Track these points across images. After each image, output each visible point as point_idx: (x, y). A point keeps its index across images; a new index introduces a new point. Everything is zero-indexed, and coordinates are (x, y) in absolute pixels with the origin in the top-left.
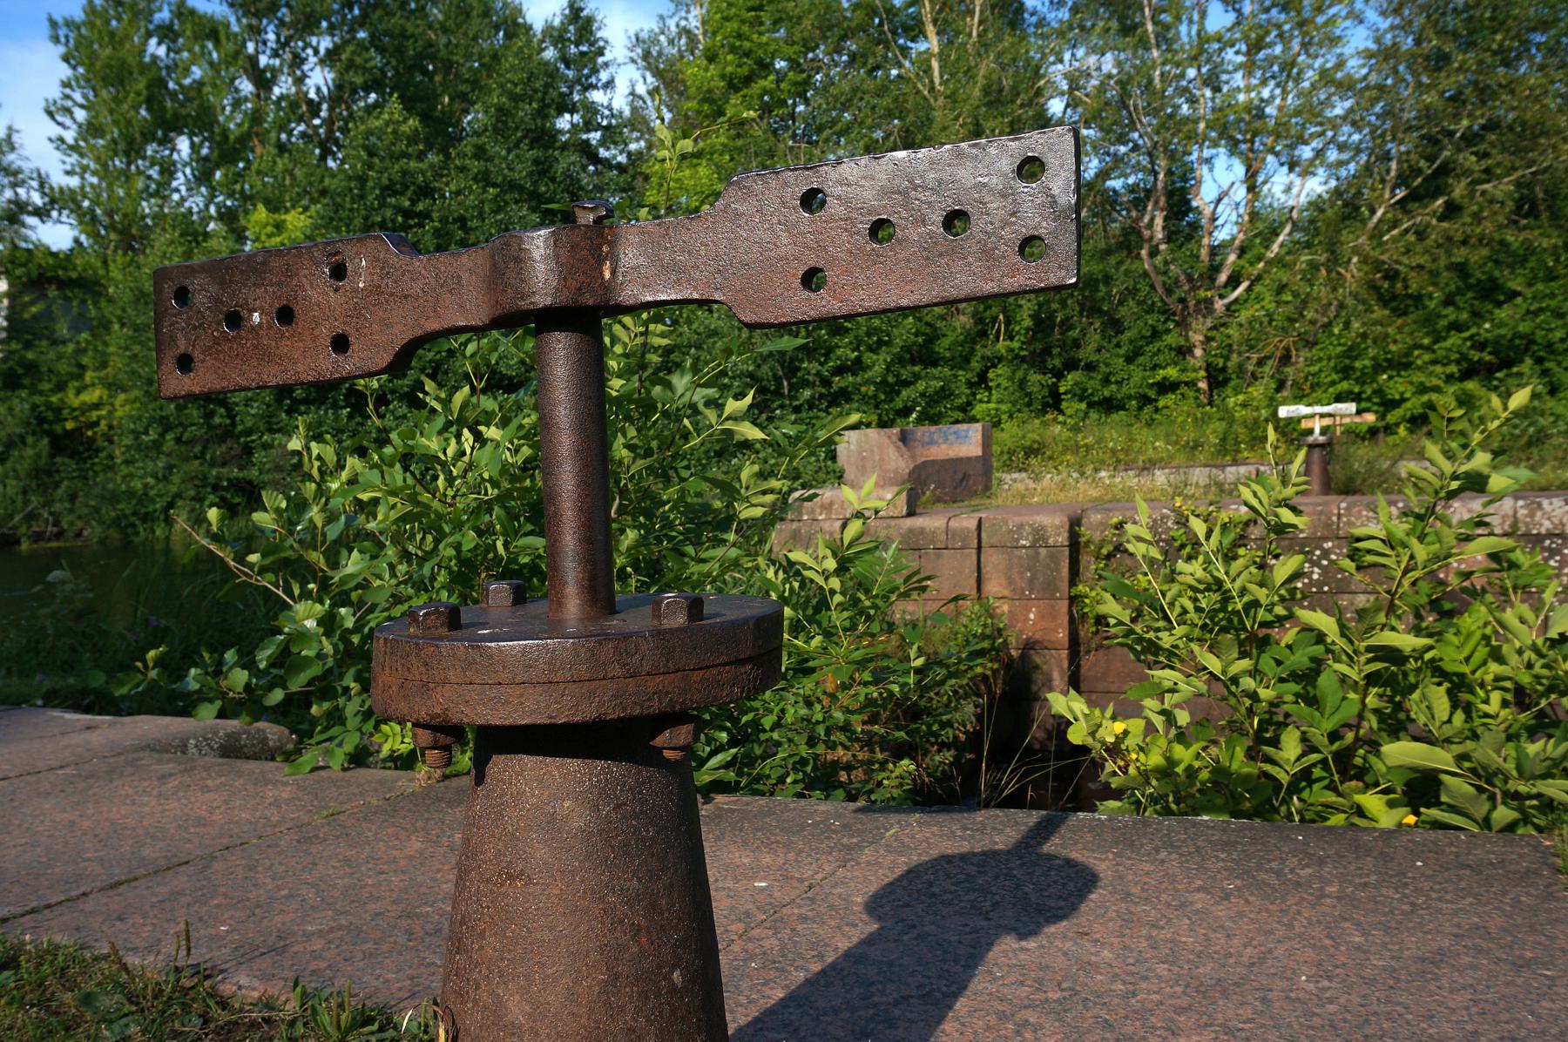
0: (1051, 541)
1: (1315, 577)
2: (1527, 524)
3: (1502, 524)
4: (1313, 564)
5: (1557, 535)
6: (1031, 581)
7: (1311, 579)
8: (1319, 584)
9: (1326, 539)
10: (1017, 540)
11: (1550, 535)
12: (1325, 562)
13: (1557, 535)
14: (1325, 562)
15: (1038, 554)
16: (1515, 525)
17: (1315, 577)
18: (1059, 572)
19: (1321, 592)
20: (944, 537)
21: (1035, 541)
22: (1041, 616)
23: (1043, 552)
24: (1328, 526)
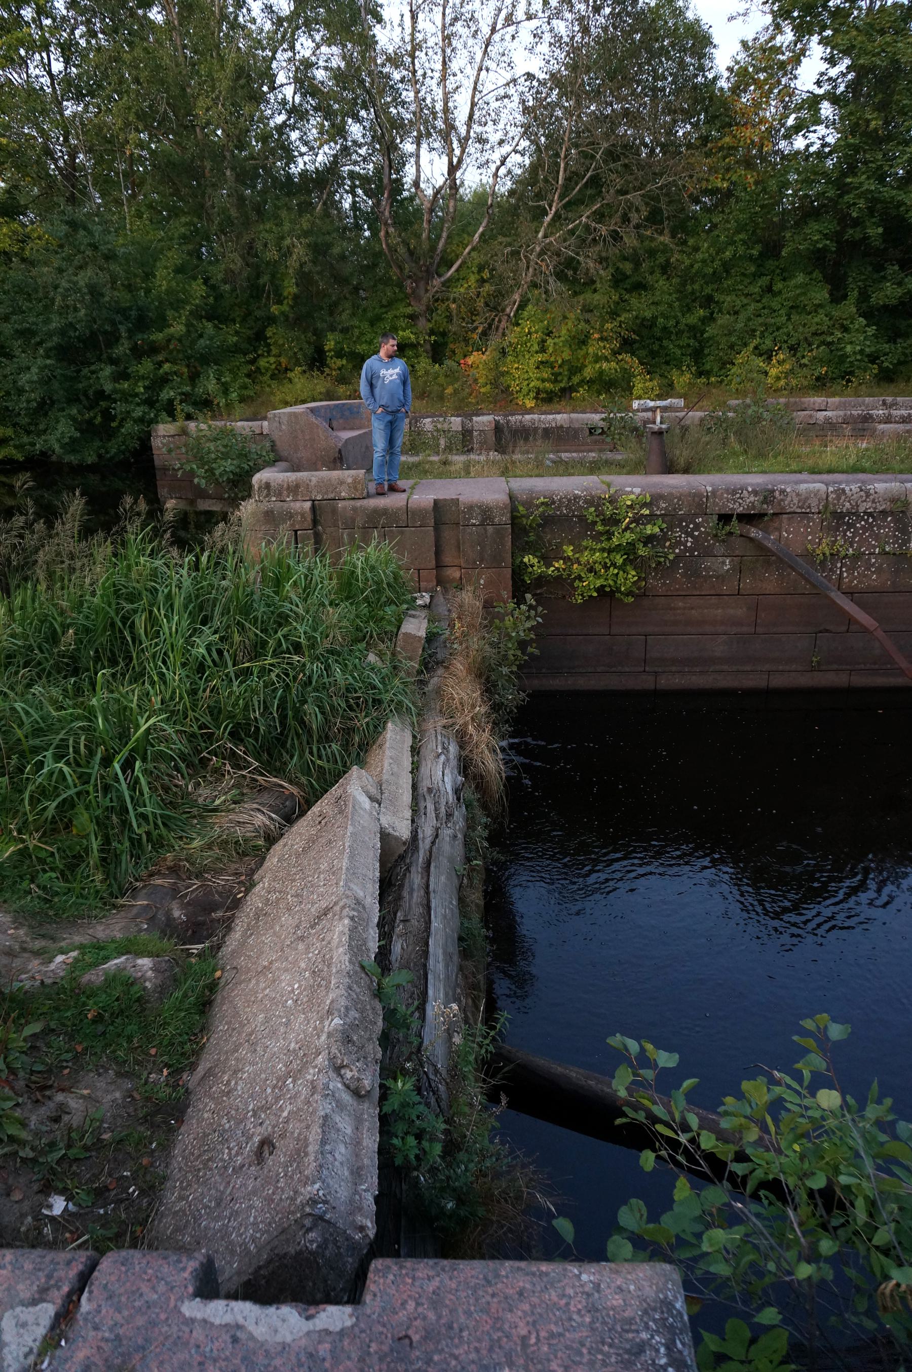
1: (689, 544)
2: (834, 505)
3: (818, 505)
4: (688, 534)
5: (853, 514)
7: (686, 546)
8: (691, 550)
9: (697, 515)
10: (469, 519)
11: (849, 513)
13: (853, 514)
15: (485, 530)
16: (826, 507)
17: (689, 544)
19: (692, 555)
23: (490, 529)
24: (699, 505)
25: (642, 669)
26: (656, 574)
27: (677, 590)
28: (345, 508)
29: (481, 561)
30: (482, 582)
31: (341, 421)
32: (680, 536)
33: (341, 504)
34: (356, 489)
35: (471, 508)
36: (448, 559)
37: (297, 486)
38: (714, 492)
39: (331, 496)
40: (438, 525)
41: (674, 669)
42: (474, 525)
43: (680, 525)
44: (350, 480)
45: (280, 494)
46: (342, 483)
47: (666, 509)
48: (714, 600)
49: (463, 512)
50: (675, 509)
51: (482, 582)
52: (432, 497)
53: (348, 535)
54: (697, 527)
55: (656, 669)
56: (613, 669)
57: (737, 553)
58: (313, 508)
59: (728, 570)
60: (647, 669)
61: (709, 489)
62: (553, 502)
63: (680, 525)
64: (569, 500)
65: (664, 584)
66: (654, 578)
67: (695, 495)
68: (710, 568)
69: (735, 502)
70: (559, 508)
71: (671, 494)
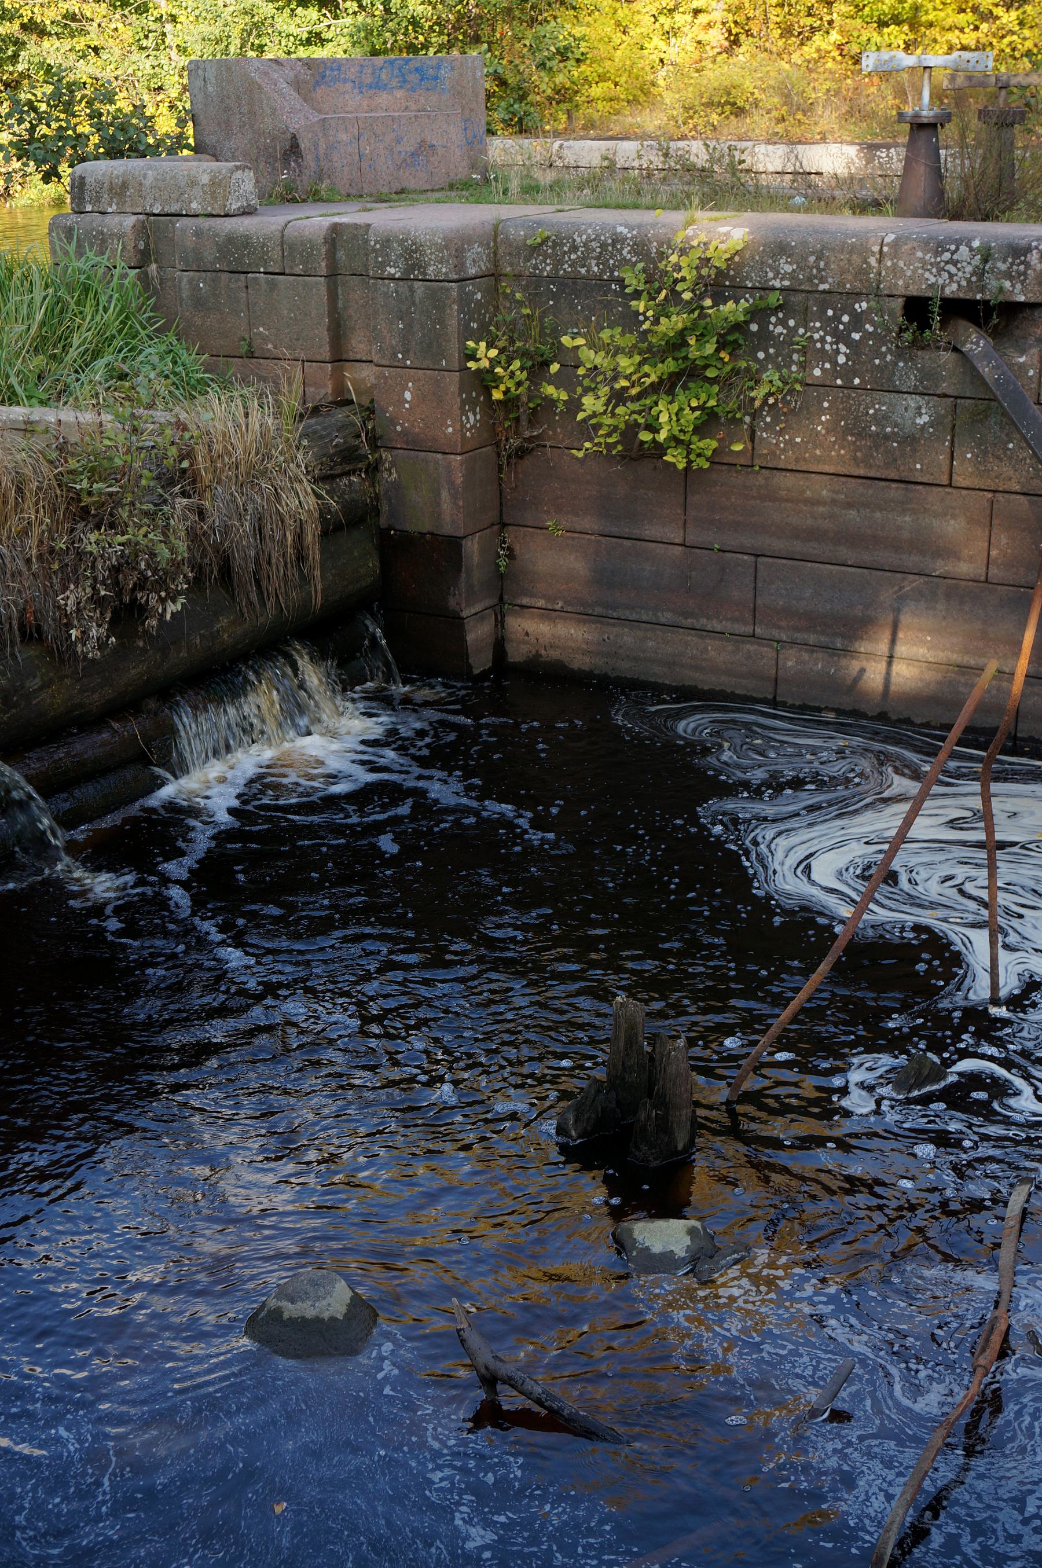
0: (431, 270)
4: (841, 337)
6: (405, 337)
7: (835, 363)
8: (847, 373)
9: (857, 295)
10: (383, 266)
12: (856, 336)
14: (856, 336)
15: (412, 290)
17: (841, 359)
18: (442, 322)
19: (848, 386)
20: (276, 254)
21: (411, 268)
22: (420, 397)
25: (749, 629)
26: (776, 420)
27: (818, 460)
28: (183, 230)
29: (406, 353)
30: (408, 396)
31: (399, 94)
32: (822, 340)
33: (180, 223)
34: (214, 198)
35: (386, 242)
36: (358, 344)
37: (124, 186)
38: (895, 245)
39: (174, 208)
40: (332, 275)
41: (812, 639)
42: (392, 278)
43: (821, 315)
44: (205, 179)
45: (98, 200)
46: (193, 183)
47: (792, 276)
48: (895, 492)
49: (374, 250)
50: (810, 279)
51: (408, 396)
52: (327, 222)
53: (190, 281)
54: (858, 320)
55: (776, 633)
56: (689, 622)
57: (944, 387)
58: (141, 230)
59: (923, 427)
60: (758, 631)
61: (890, 238)
62: (574, 248)
63: (821, 315)
64: (603, 246)
65: (790, 443)
66: (768, 427)
67: (852, 249)
68: (885, 417)
69: (941, 270)
70: (583, 261)
71: (804, 243)
